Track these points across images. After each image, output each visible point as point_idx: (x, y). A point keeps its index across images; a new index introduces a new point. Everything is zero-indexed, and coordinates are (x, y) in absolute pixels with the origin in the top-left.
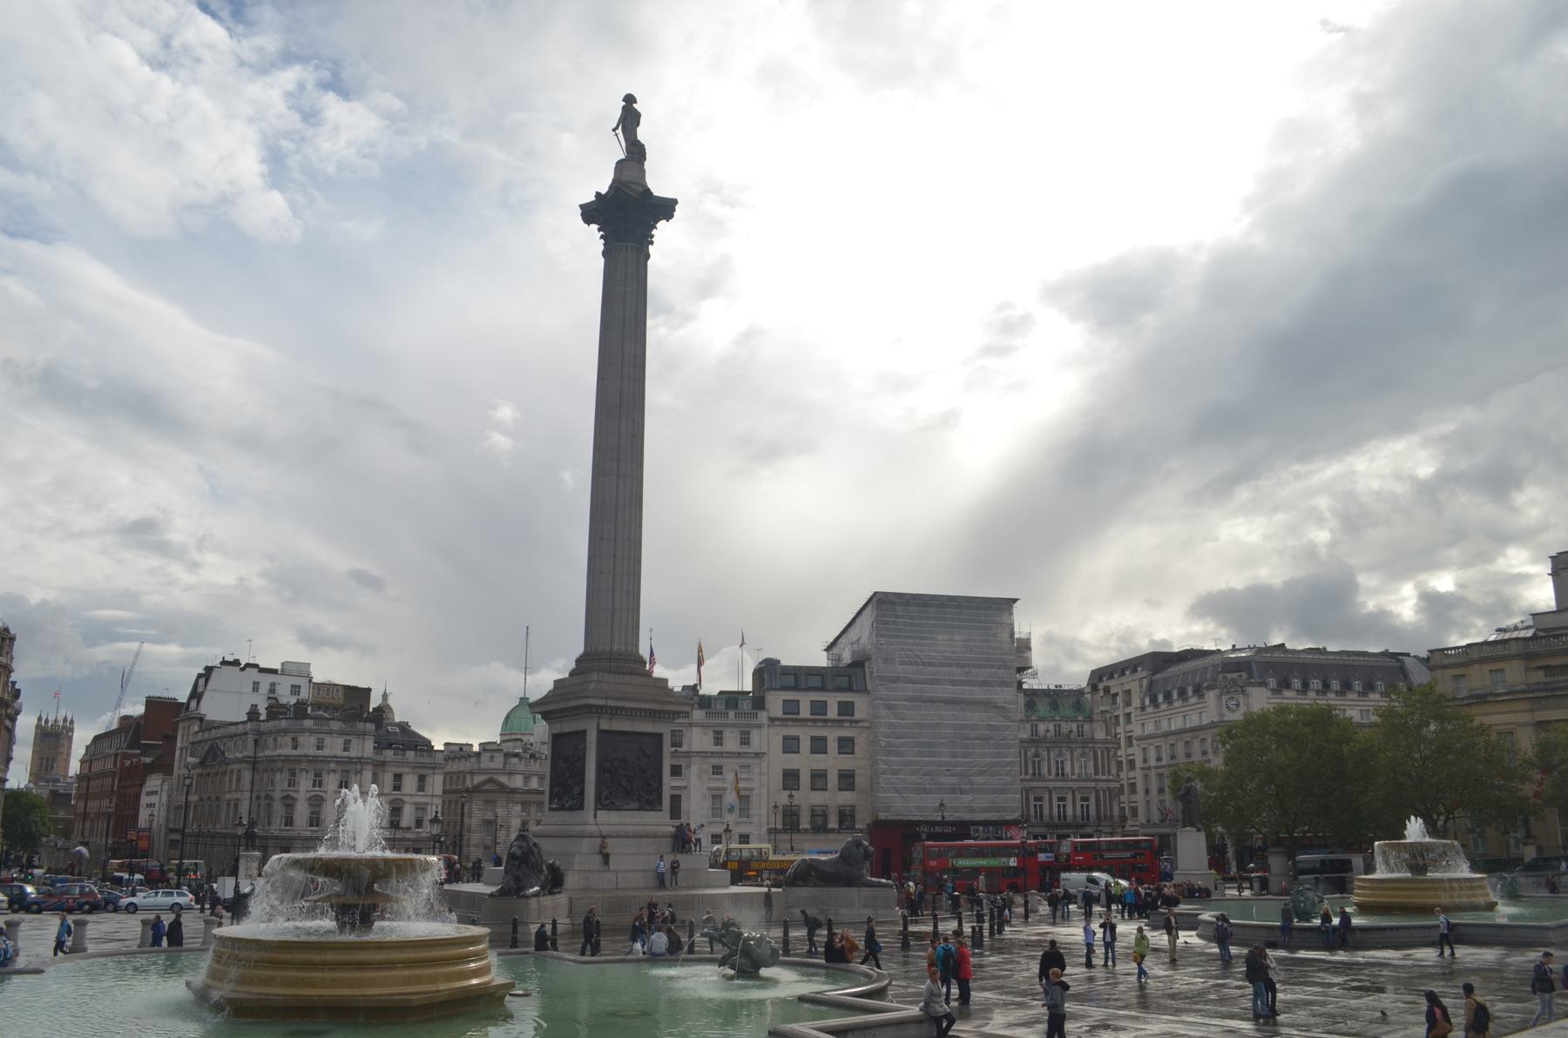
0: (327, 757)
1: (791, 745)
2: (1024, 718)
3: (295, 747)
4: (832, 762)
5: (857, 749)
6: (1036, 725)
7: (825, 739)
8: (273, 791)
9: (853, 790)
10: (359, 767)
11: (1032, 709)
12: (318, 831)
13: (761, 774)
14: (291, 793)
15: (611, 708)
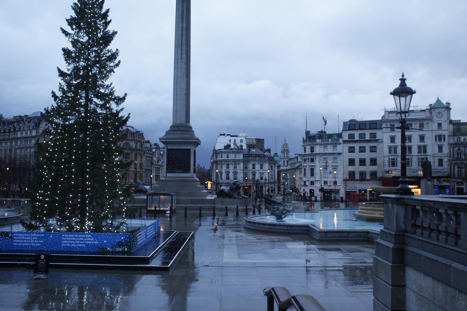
0: (229, 160)
1: (351, 150)
2: (452, 134)
3: (222, 158)
4: (368, 155)
5: (377, 150)
6: (460, 138)
7: (365, 147)
8: (223, 170)
9: (376, 165)
10: (239, 162)
11: (458, 131)
12: (228, 181)
13: (341, 160)
14: (221, 170)
15: (170, 142)
